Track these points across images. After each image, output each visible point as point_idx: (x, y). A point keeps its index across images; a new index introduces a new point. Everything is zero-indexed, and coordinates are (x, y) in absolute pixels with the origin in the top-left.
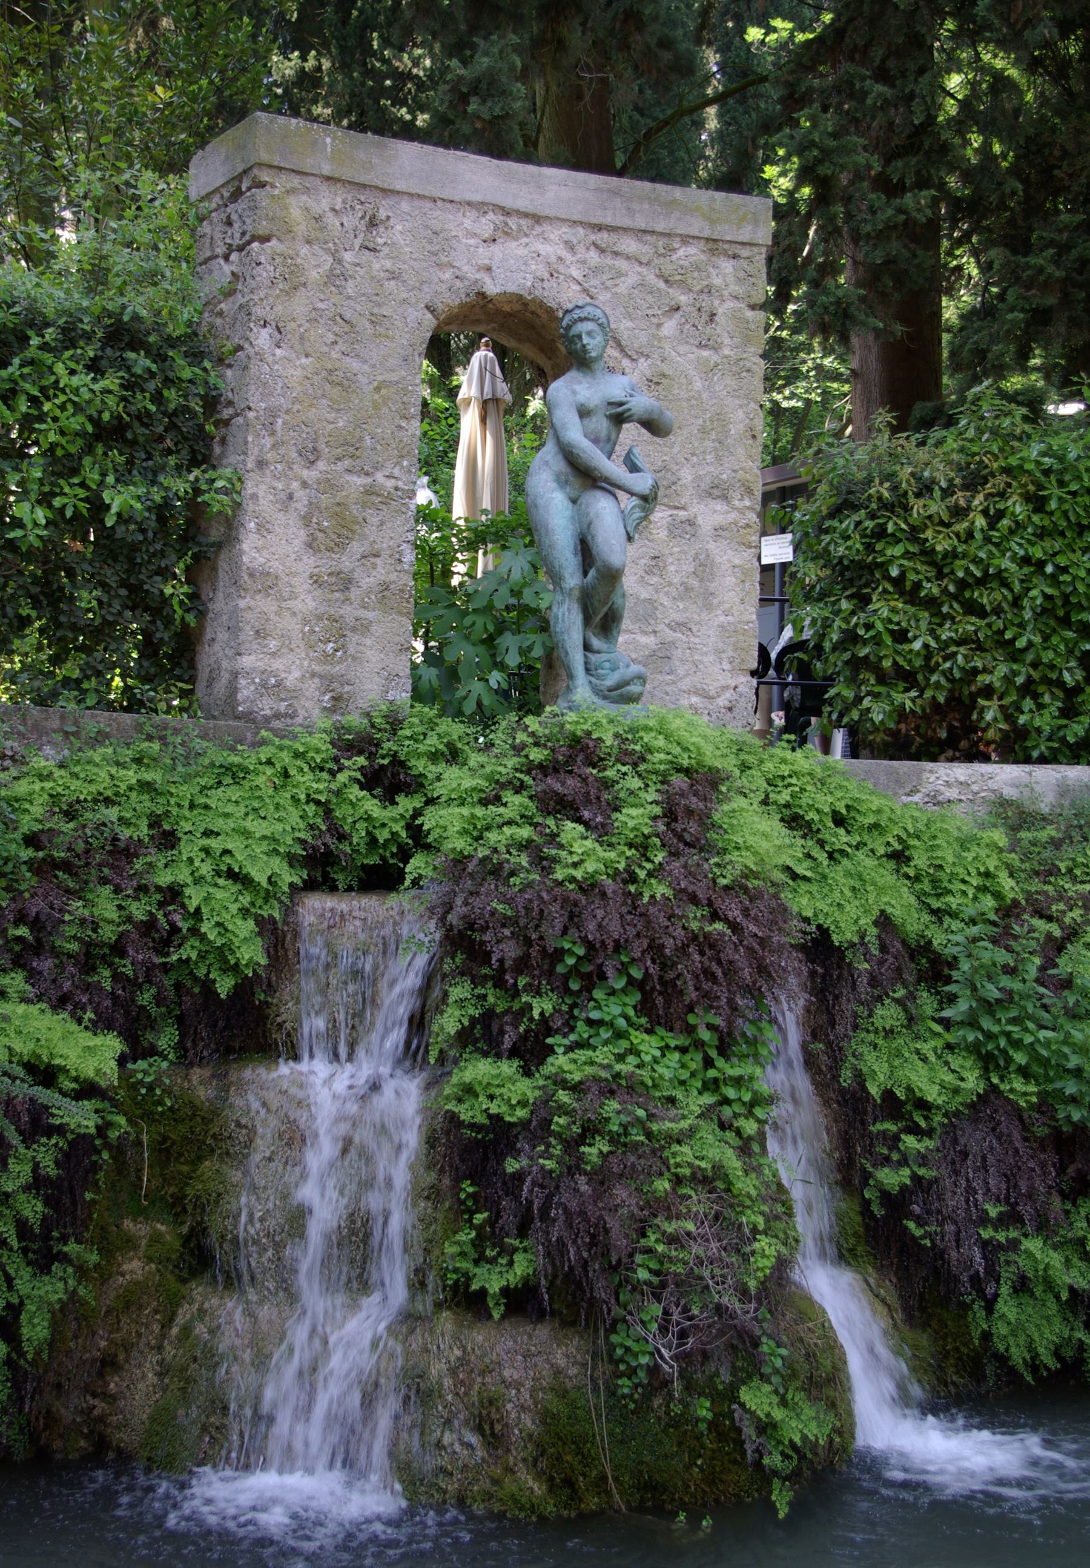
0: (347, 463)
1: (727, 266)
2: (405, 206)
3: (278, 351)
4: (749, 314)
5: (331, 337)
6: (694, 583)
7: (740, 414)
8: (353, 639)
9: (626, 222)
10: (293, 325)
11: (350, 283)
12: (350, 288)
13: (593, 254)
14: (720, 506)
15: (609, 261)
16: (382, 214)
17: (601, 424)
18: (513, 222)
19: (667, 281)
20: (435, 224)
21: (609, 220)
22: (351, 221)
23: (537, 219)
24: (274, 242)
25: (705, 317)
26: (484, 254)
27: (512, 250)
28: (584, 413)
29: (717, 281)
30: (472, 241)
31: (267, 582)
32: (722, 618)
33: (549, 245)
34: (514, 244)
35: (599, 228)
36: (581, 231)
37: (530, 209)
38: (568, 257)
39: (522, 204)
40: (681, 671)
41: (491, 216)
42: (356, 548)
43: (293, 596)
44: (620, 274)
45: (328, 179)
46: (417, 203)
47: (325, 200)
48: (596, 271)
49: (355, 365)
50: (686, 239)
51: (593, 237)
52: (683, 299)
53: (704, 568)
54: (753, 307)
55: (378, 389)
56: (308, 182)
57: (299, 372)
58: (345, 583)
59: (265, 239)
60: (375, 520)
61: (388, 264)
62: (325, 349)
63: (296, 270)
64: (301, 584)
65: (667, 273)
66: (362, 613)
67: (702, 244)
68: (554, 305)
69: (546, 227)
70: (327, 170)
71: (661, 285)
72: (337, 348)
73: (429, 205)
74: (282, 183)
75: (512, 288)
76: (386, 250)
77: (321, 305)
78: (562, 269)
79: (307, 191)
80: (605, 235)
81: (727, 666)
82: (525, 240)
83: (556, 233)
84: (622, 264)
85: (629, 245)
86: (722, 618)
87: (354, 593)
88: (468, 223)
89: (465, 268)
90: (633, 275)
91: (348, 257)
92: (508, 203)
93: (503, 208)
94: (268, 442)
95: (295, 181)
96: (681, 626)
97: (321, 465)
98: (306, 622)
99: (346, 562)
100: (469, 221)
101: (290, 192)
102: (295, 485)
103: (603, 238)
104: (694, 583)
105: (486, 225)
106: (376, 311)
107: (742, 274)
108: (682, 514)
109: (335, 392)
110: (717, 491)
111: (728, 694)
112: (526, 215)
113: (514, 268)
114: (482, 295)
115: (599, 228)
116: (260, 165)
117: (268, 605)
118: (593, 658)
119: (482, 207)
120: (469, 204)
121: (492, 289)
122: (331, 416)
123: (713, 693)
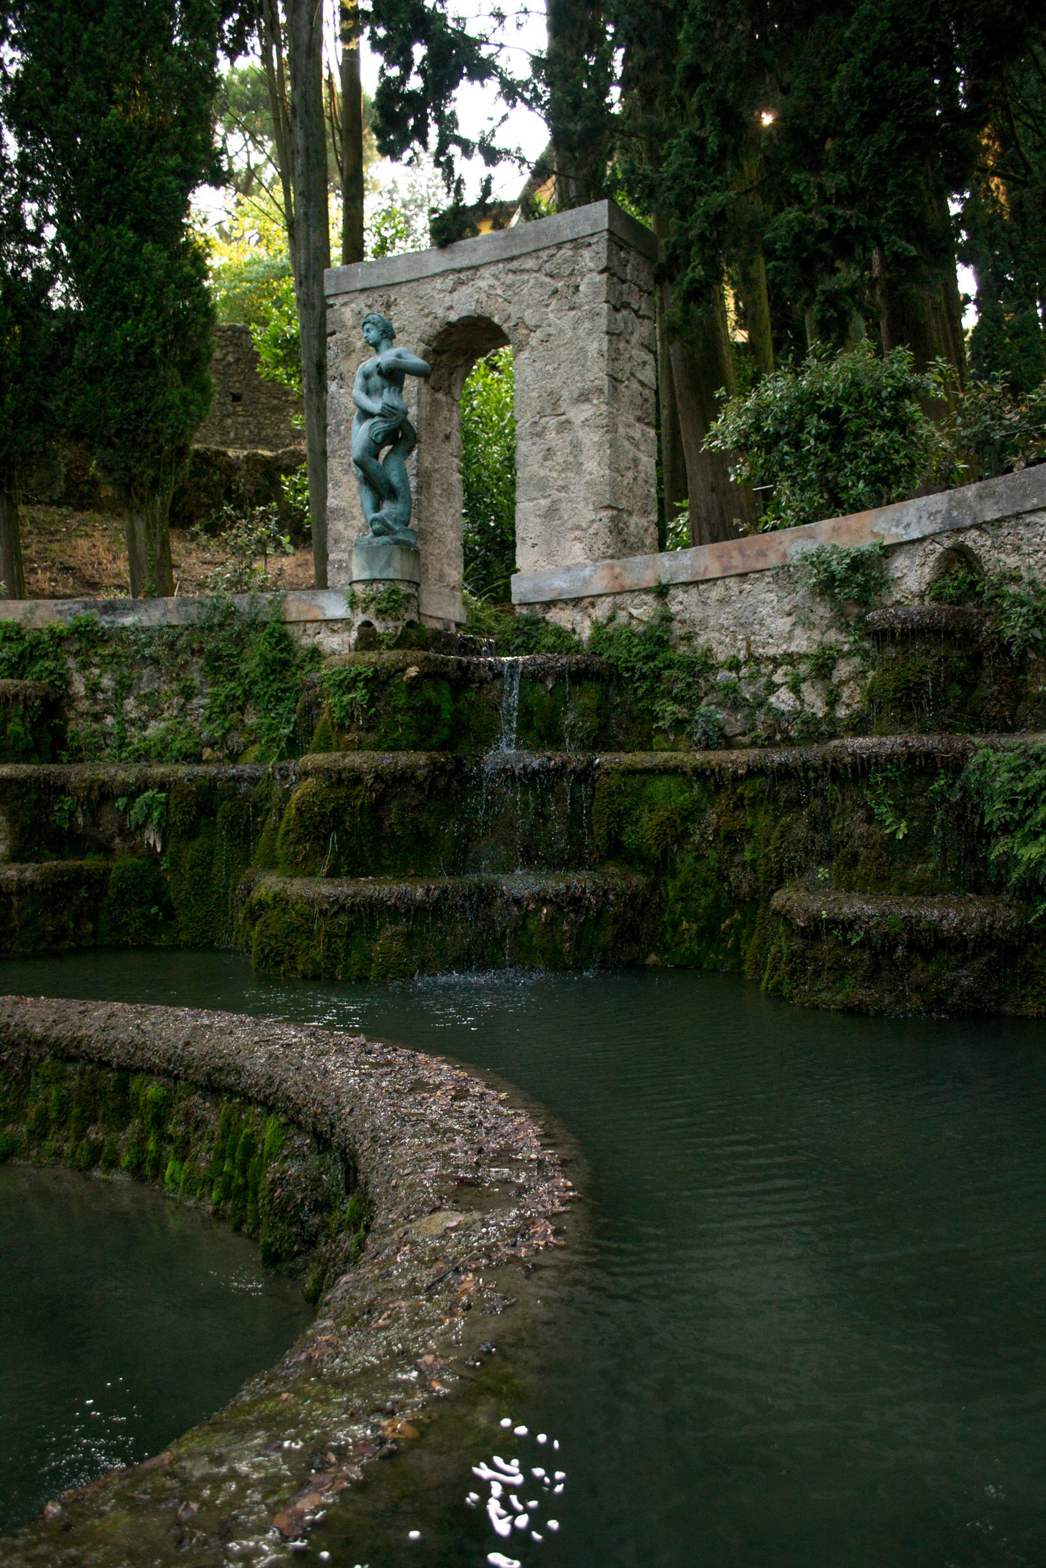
1: (586, 253)
2: (404, 289)
6: (571, 459)
7: (595, 345)
9: (525, 250)
13: (511, 276)
14: (585, 406)
20: (421, 293)
21: (516, 252)
23: (476, 268)
25: (571, 289)
26: (448, 300)
27: (465, 290)
31: (341, 514)
32: (588, 478)
33: (485, 281)
34: (465, 287)
36: (501, 265)
38: (497, 283)
40: (566, 517)
43: (353, 518)
44: (524, 282)
45: (363, 290)
47: (361, 303)
50: (559, 246)
53: (576, 447)
67: (568, 246)
70: (359, 286)
71: (548, 280)
74: (341, 300)
75: (464, 314)
78: (492, 292)
79: (352, 301)
81: (591, 507)
83: (485, 272)
84: (525, 277)
85: (530, 263)
88: (438, 286)
90: (532, 278)
92: (457, 265)
96: (563, 488)
98: (360, 530)
100: (438, 283)
101: (345, 304)
103: (509, 266)
104: (571, 459)
105: (450, 281)
108: (563, 418)
110: (583, 397)
111: (595, 526)
112: (469, 269)
114: (449, 324)
117: (340, 526)
119: (443, 274)
121: (453, 317)
123: (584, 525)
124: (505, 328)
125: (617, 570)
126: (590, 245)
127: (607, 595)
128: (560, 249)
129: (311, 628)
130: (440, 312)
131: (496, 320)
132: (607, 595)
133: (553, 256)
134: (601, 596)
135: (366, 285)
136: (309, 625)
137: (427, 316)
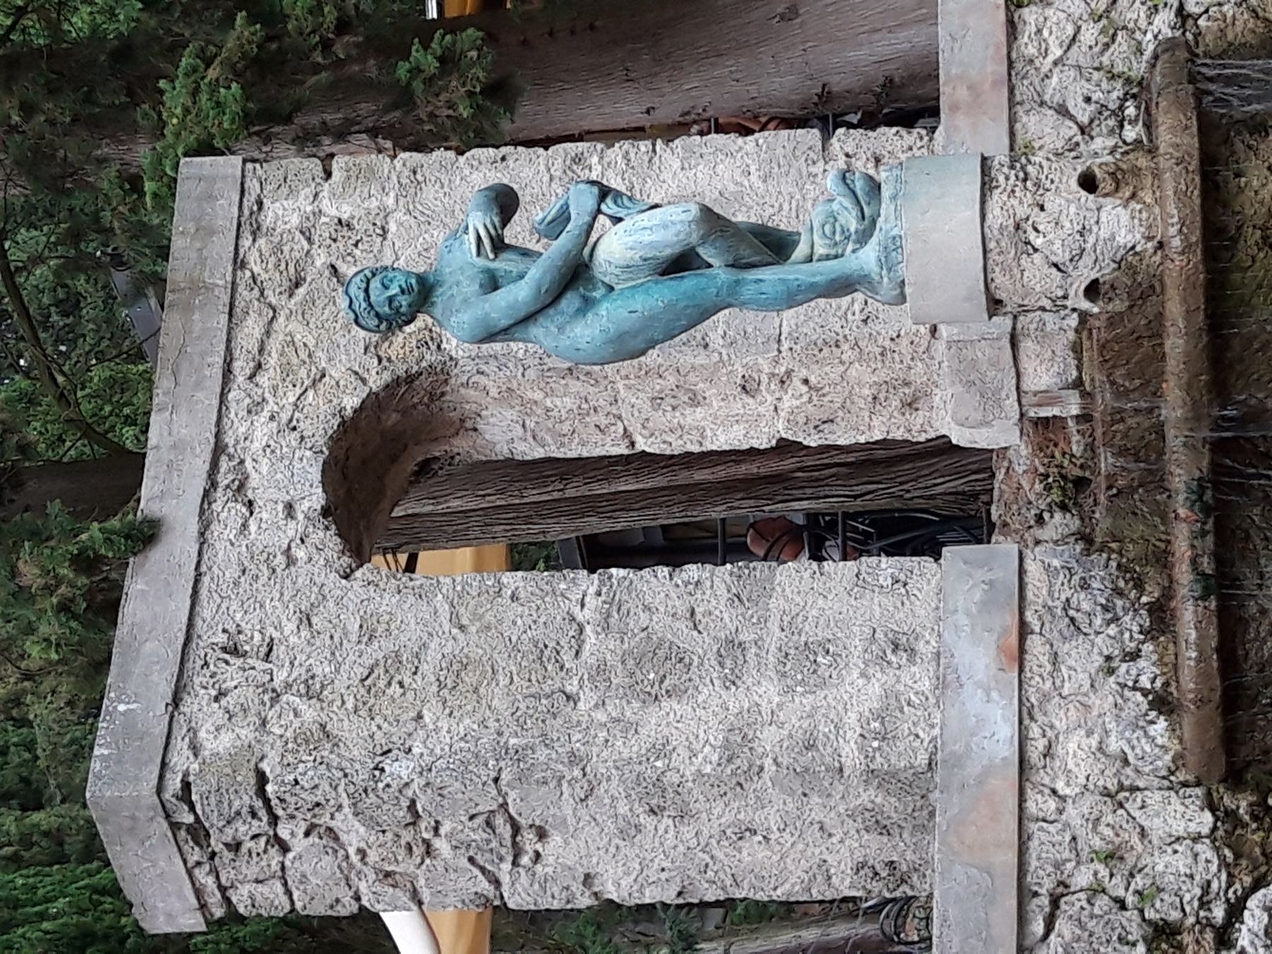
0: (567, 657)
1: (272, 211)
2: (206, 611)
3: (416, 751)
4: (337, 175)
5: (395, 689)
8: (811, 632)
10: (379, 735)
11: (318, 671)
12: (323, 669)
13: (263, 379)
15: (272, 360)
16: (221, 639)
17: (504, 264)
18: (223, 480)
19: (297, 285)
20: (232, 573)
21: (218, 360)
22: (231, 674)
23: (219, 449)
24: (265, 766)
27: (260, 476)
28: (492, 283)
29: (295, 220)
30: (253, 527)
33: (254, 434)
35: (228, 372)
37: (208, 456)
39: (201, 465)
41: (217, 507)
42: (683, 635)
46: (204, 592)
48: (287, 370)
49: (432, 656)
50: (239, 263)
51: (240, 379)
52: (321, 260)
54: (328, 174)
55: (462, 628)
56: (180, 731)
57: (444, 724)
58: (733, 646)
59: (262, 779)
60: (644, 618)
61: (289, 627)
62: (410, 695)
63: (303, 739)
64: (736, 701)
65: (286, 284)
66: (774, 626)
68: (336, 422)
69: (229, 440)
71: (301, 291)
72: (407, 681)
73: (206, 580)
74: (181, 759)
75: (315, 473)
76: (270, 631)
77: (350, 705)
78: (285, 417)
80: (237, 365)
82: (249, 464)
84: (274, 345)
86: (753, 178)
87: (745, 636)
89: (291, 533)
91: (280, 677)
92: (200, 483)
93: (206, 494)
94: (542, 754)
95: (181, 745)
97: (572, 688)
98: (789, 690)
99: (702, 645)
101: (195, 749)
102: (600, 716)
103: (241, 367)
105: (228, 513)
106: (354, 638)
107: (285, 190)
109: (469, 678)
113: (289, 476)
114: (326, 512)
115: (228, 372)
116: (159, 790)
118: (820, 250)
120: (202, 534)
121: (316, 498)
122: (504, 681)
124: (376, 381)
125: (962, 93)
126: (260, 204)
127: (1012, 120)
128: (243, 265)
129: (1038, 803)
130: (292, 529)
131: (351, 402)
132: (1012, 120)
133: (253, 277)
134: (1012, 134)
135: (167, 691)
136: (1031, 807)
137: (291, 561)
